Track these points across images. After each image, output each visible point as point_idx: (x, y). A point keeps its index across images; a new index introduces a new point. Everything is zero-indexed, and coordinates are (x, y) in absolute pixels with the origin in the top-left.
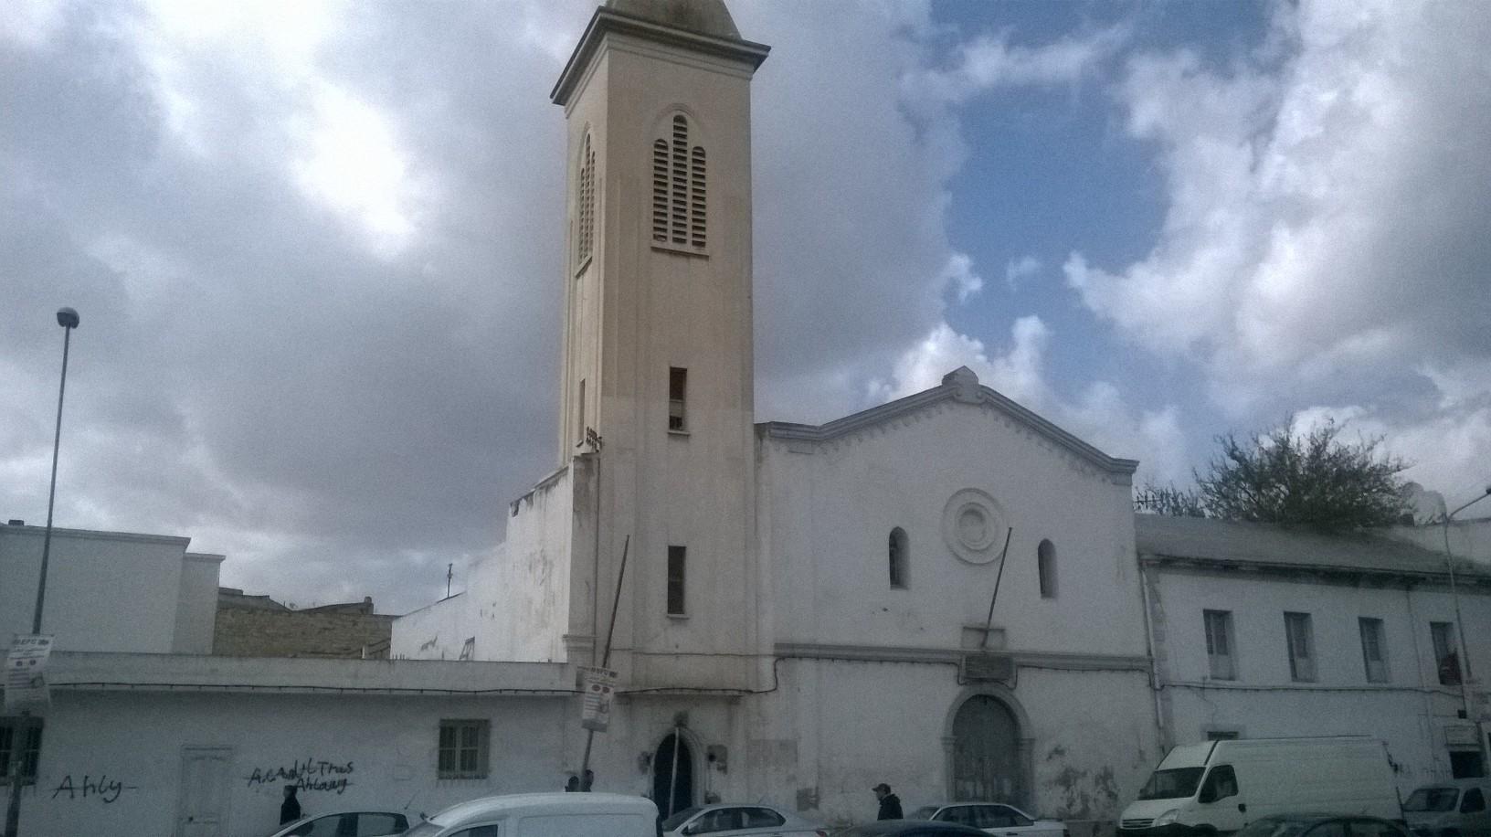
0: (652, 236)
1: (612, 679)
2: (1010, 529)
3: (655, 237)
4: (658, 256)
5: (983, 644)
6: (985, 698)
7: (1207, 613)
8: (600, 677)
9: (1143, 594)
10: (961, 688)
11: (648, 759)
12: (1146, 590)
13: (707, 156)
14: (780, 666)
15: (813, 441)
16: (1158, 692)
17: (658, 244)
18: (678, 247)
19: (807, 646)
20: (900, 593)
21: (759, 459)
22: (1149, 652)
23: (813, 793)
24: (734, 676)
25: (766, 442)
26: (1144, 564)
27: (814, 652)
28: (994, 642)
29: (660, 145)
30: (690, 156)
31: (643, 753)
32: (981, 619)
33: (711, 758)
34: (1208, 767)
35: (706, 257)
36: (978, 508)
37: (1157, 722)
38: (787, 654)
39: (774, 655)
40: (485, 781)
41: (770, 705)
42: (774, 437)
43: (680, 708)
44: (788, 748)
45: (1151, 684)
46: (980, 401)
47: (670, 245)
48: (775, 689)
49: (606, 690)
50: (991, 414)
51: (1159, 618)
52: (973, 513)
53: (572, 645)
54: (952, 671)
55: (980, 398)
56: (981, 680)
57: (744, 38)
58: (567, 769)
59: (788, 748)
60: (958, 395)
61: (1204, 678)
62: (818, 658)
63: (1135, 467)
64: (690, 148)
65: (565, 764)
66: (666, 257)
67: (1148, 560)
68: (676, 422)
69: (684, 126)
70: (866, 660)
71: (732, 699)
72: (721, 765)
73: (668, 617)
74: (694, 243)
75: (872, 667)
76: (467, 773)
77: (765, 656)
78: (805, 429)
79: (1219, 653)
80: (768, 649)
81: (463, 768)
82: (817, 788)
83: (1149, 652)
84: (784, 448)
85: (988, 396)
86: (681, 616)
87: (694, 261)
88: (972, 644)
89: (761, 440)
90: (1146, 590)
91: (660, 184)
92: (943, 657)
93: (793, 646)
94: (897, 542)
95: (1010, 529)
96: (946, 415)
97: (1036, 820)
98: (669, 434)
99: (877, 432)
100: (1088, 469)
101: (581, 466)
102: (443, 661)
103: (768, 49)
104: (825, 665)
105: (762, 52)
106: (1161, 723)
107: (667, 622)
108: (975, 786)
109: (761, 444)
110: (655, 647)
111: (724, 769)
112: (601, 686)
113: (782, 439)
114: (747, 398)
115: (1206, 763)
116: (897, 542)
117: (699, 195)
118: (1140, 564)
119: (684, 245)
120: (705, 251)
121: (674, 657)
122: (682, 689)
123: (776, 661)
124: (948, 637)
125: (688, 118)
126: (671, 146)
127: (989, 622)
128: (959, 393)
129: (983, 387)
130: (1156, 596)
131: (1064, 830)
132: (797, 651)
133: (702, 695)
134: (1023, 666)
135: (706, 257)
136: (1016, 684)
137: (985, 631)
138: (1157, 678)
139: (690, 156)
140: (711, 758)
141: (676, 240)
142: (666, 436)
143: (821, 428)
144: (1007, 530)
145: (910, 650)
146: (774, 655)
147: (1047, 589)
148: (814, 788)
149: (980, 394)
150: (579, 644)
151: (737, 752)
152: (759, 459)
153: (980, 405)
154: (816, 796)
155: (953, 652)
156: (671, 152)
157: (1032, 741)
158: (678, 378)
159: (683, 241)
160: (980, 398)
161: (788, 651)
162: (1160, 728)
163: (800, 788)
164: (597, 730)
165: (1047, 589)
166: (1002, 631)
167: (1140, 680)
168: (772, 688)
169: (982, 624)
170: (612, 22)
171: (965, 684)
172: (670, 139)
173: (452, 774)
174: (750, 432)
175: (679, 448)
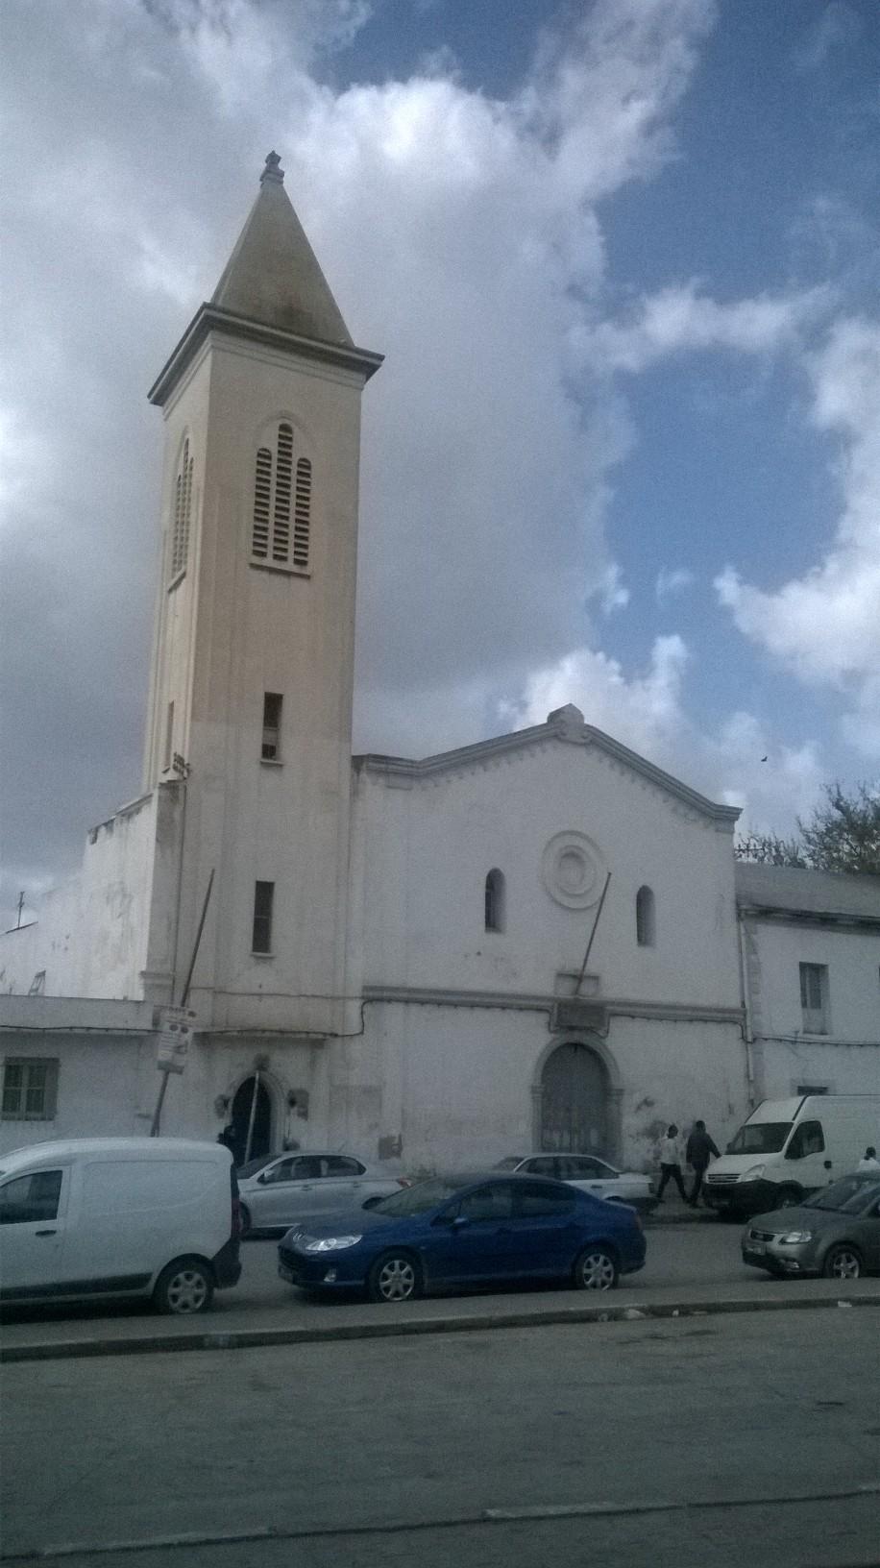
0: (251, 552)
1: (190, 1019)
2: (610, 874)
3: (256, 553)
4: (256, 573)
5: (576, 992)
6: (577, 1046)
7: (803, 966)
8: (180, 1016)
9: (740, 944)
11: (226, 1103)
12: (743, 939)
13: (313, 469)
14: (368, 1008)
15: (410, 776)
16: (749, 1045)
17: (256, 560)
18: (276, 564)
19: (396, 989)
20: (493, 937)
21: (355, 793)
22: (743, 1003)
23: (396, 1141)
24: (319, 1017)
25: (364, 775)
26: (743, 915)
27: (405, 995)
28: (587, 989)
29: (264, 455)
30: (294, 468)
31: (221, 1097)
33: (292, 1103)
34: (796, 1123)
35: (308, 577)
36: (575, 851)
37: (748, 1076)
38: (375, 996)
39: (363, 998)
40: (51, 1122)
41: (356, 1049)
42: (370, 771)
43: (263, 1050)
44: (373, 1093)
45: (743, 1038)
46: (583, 741)
47: (269, 561)
48: (362, 1033)
49: (185, 1030)
50: (596, 754)
51: (755, 969)
52: (572, 856)
53: (149, 982)
54: (543, 1018)
55: (584, 738)
56: (572, 1028)
57: (358, 343)
58: (138, 1112)
59: (373, 1093)
60: (564, 734)
61: (797, 1032)
62: (407, 1002)
63: (739, 814)
64: (295, 459)
65: (137, 1107)
66: (265, 575)
67: (746, 910)
68: (269, 751)
69: (290, 435)
70: (456, 1005)
71: (316, 1042)
72: (302, 1110)
73: (252, 955)
74: (297, 562)
75: (464, 1014)
76: (32, 1114)
77: (352, 998)
78: (404, 763)
79: (813, 1007)
80: (356, 990)
81: (28, 1109)
82: (400, 1136)
83: (743, 1003)
84: (381, 781)
87: (296, 582)
88: (565, 991)
89: (358, 773)
90: (743, 939)
91: (261, 495)
92: (536, 1003)
93: (382, 989)
94: (494, 884)
95: (610, 874)
96: (552, 755)
97: (622, 1173)
98: (262, 763)
99: (479, 769)
101: (166, 793)
102: (10, 995)
103: (381, 358)
104: (414, 1008)
105: (375, 361)
106: (752, 1078)
107: (252, 960)
108: (562, 1136)
109: (358, 779)
111: (304, 1115)
112: (179, 1026)
113: (379, 772)
114: (343, 727)
115: (794, 1119)
116: (494, 884)
117: (303, 512)
118: (739, 915)
119: (285, 563)
120: (306, 571)
121: (256, 997)
122: (264, 1031)
123: (364, 1004)
124: (541, 983)
125: (296, 430)
126: (275, 456)
127: (584, 966)
129: (588, 726)
130: (753, 949)
131: (650, 1184)
132: (385, 994)
133: (283, 1038)
134: (615, 1015)
135: (308, 577)
137: (579, 978)
138: (749, 1029)
139: (294, 468)
140: (292, 1103)
141: (276, 557)
142: (257, 766)
143: (420, 762)
144: (606, 875)
145: (503, 996)
146: (363, 998)
148: (397, 1136)
149: (586, 734)
150: (157, 982)
151: (319, 1095)
152: (355, 793)
153: (584, 745)
154: (400, 1146)
155: (549, 999)
156: (275, 464)
157: (621, 1092)
158: (273, 705)
159: (284, 559)
160: (584, 738)
161: (377, 994)
162: (751, 1082)
163: (385, 1136)
164: (173, 1072)
166: (596, 978)
167: (734, 1031)
168: (358, 1032)
169: (577, 970)
170: (214, 319)
171: (555, 1032)
172: (274, 449)
173: (16, 1115)
174: (347, 765)
175: (271, 778)
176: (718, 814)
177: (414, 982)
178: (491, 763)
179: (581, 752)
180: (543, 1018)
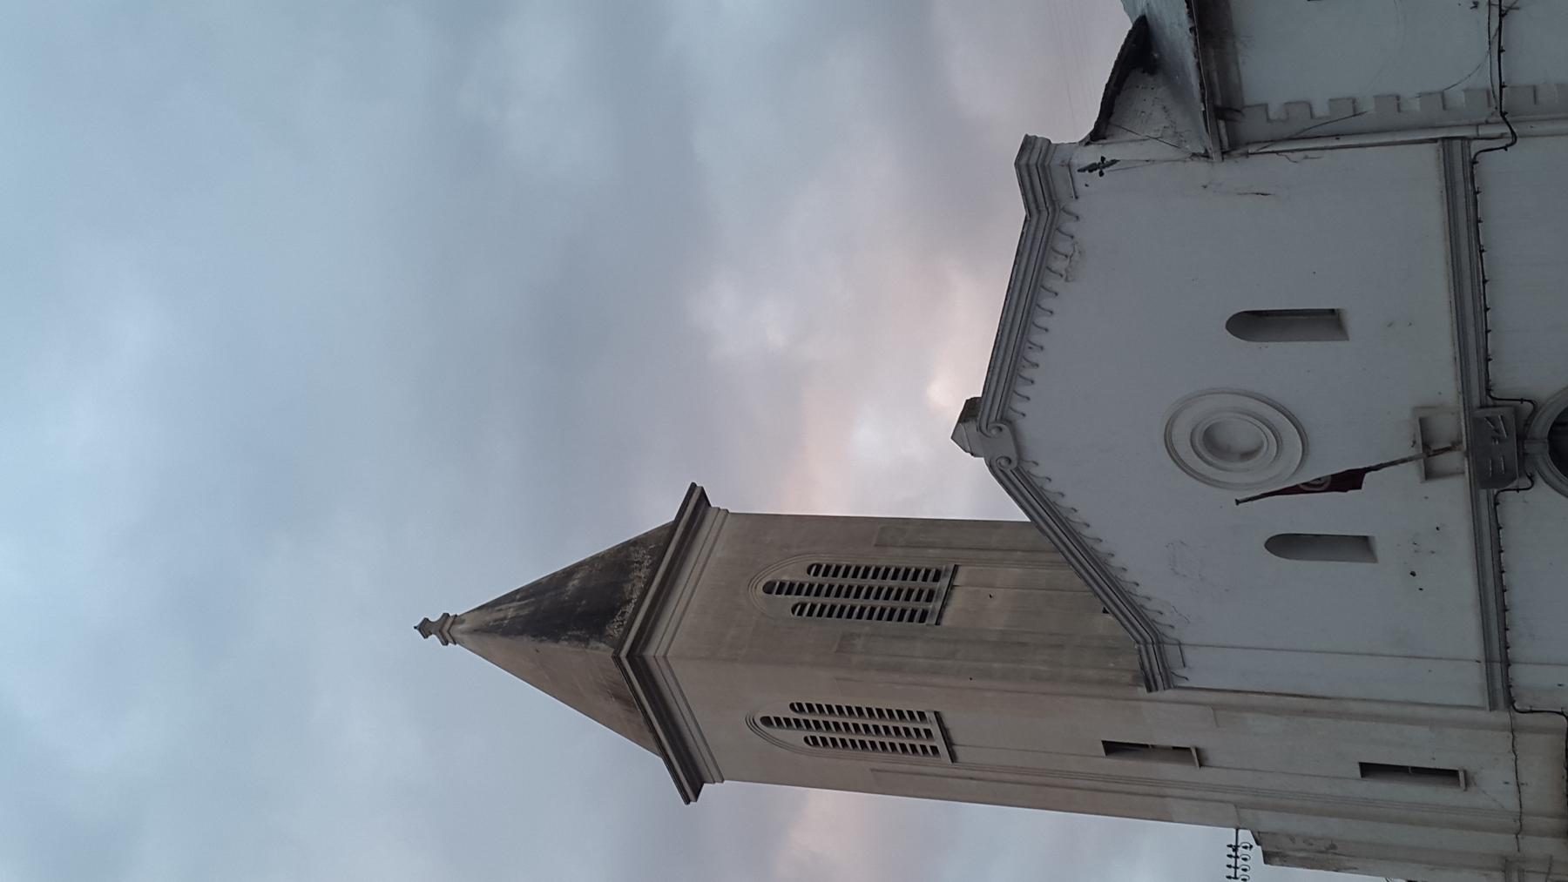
2: (1238, 502)
10: (1539, 480)
19: (1490, 677)
27: (1497, 667)
28: (1450, 426)
32: (1412, 471)
62: (1507, 663)
66: (958, 750)
70: (1503, 610)
80: (1502, 717)
85: (993, 418)
86: (1461, 775)
87: (948, 723)
95: (1238, 502)
98: (1201, 765)
99: (1115, 562)
100: (1063, 246)
110: (1511, 803)
121: (1523, 788)
128: (1003, 462)
136: (1522, 400)
147: (1328, 322)
165: (1328, 322)
167: (1496, 168)
171: (1531, 478)
176: (1043, 208)
177: (1474, 649)
178: (1102, 548)
179: (1024, 425)
180: (1513, 504)
